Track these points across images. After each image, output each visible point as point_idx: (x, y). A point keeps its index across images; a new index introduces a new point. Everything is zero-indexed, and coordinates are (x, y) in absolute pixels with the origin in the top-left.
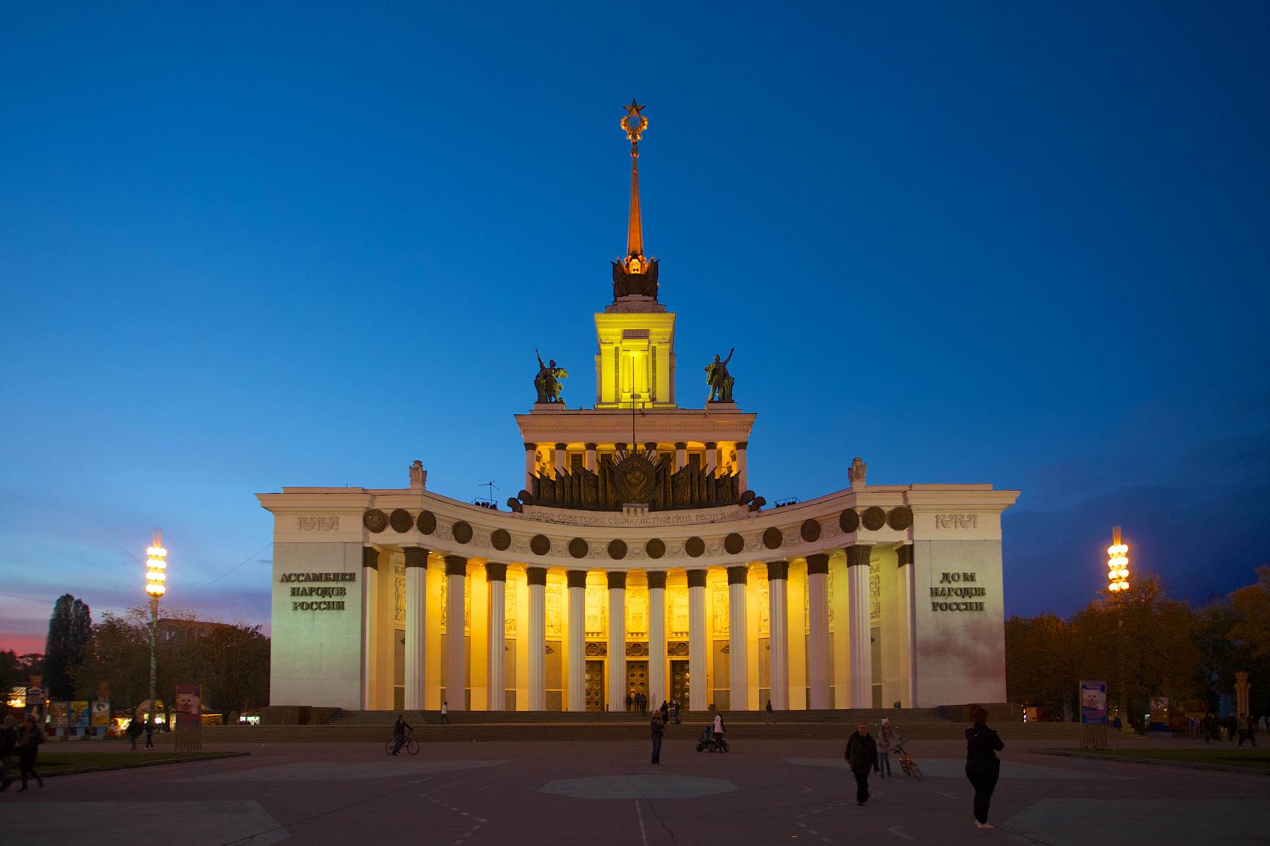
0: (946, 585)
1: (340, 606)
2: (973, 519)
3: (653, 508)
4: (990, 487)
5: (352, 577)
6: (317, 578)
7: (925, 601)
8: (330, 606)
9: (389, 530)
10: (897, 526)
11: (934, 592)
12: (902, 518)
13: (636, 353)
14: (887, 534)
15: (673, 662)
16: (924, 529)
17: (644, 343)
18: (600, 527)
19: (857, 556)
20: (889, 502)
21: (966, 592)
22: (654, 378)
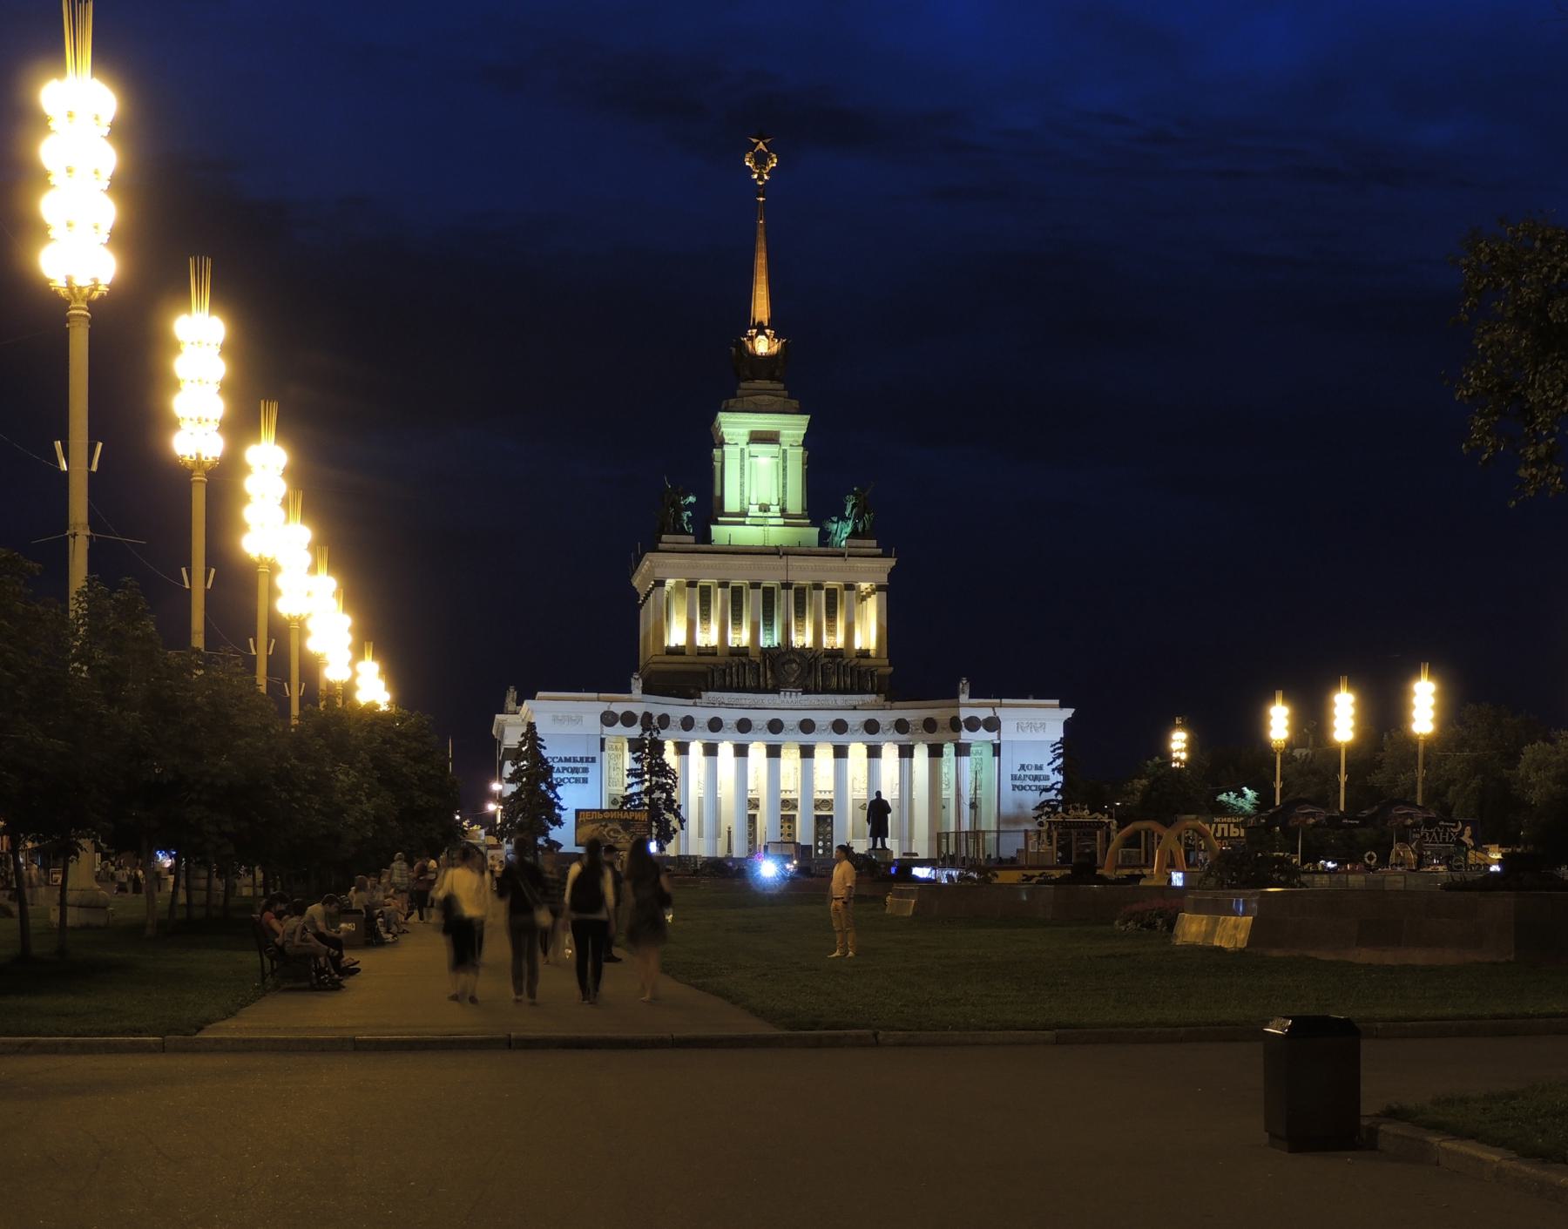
0: (1023, 773)
1: (585, 781)
2: (1043, 726)
3: (806, 691)
4: (1057, 702)
5: (593, 760)
6: (568, 760)
7: (1007, 783)
8: (577, 780)
9: (619, 724)
10: (989, 729)
11: (1014, 777)
12: (993, 725)
13: (764, 460)
14: (982, 734)
15: (818, 817)
16: (1008, 733)
17: (773, 449)
18: (760, 708)
19: (962, 750)
20: (983, 714)
21: (1036, 778)
22: (784, 486)
